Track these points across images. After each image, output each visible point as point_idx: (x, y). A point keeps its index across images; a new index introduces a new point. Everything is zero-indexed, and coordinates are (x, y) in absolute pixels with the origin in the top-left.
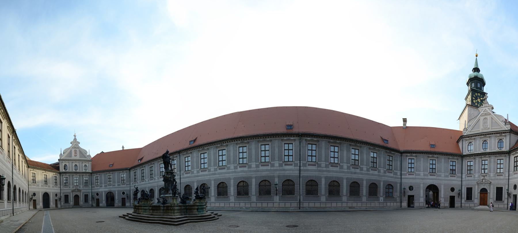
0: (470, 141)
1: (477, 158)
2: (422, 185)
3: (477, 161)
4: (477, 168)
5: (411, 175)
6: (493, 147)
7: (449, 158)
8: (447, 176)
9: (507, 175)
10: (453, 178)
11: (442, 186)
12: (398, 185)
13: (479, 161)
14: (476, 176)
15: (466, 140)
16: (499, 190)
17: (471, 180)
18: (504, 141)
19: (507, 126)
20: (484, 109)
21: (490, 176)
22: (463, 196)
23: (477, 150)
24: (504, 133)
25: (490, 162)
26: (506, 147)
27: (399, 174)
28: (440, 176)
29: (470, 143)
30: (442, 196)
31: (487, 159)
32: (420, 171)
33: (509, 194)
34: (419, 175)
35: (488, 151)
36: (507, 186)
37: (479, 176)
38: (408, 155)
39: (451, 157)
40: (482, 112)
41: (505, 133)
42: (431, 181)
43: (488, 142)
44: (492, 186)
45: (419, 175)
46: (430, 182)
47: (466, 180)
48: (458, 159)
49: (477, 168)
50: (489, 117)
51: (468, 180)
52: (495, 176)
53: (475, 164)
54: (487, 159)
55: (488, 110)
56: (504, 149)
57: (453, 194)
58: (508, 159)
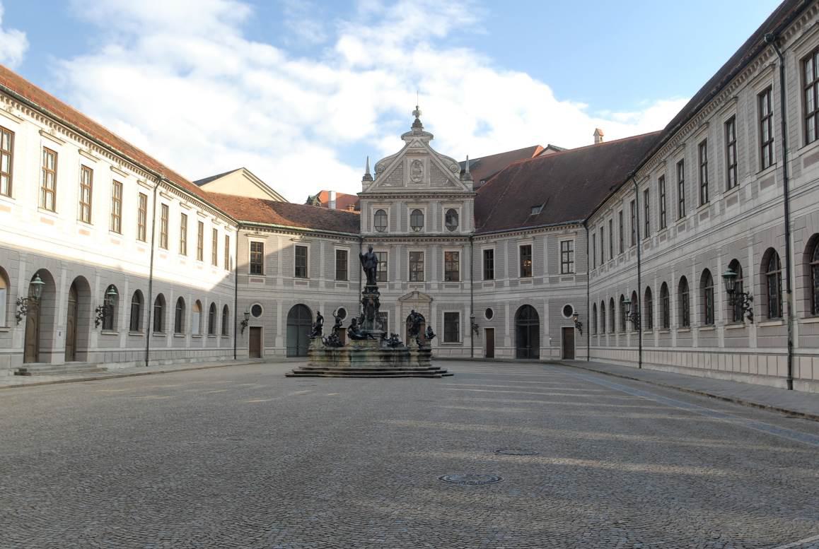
1: (398, 249)
7: (333, 244)
9: (469, 286)
16: (451, 320)
21: (428, 287)
33: (475, 328)
37: (404, 287)
44: (434, 310)
46: (296, 299)
52: (440, 287)
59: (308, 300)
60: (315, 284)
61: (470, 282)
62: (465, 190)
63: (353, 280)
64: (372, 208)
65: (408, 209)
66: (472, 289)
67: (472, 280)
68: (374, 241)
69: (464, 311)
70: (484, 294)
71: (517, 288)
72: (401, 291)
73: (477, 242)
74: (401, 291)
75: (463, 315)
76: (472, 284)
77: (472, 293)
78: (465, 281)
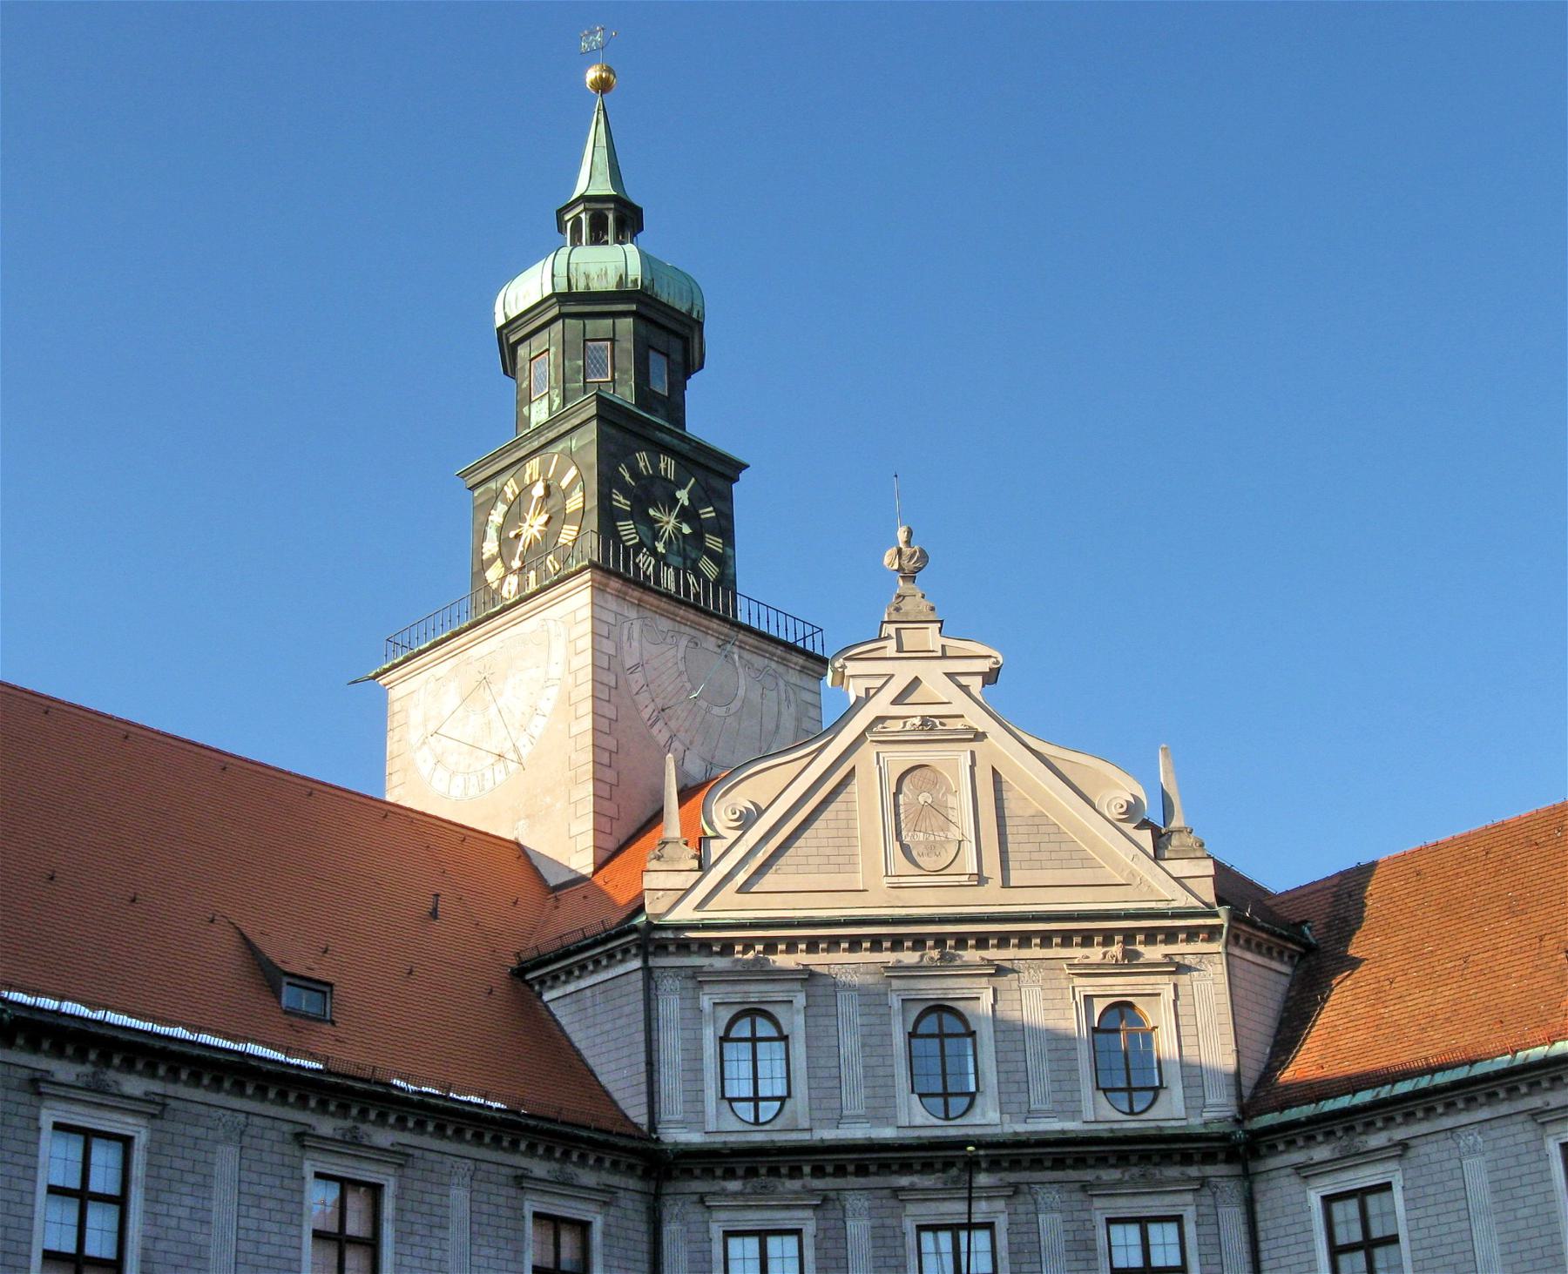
0: (755, 993)
1: (856, 1203)
3: (858, 1229)
7: (520, 1180)
15: (697, 978)
19: (1179, 868)
20: (904, 673)
23: (854, 1099)
29: (753, 1012)
35: (988, 1119)
38: (65, 1071)
39: (539, 1168)
40: (881, 705)
41: (1171, 936)
48: (607, 1197)
50: (953, 761)
55: (949, 691)
58: (1232, 1219)
62: (1183, 900)
64: (706, 1002)
68: (730, 1174)
73: (1273, 1162)
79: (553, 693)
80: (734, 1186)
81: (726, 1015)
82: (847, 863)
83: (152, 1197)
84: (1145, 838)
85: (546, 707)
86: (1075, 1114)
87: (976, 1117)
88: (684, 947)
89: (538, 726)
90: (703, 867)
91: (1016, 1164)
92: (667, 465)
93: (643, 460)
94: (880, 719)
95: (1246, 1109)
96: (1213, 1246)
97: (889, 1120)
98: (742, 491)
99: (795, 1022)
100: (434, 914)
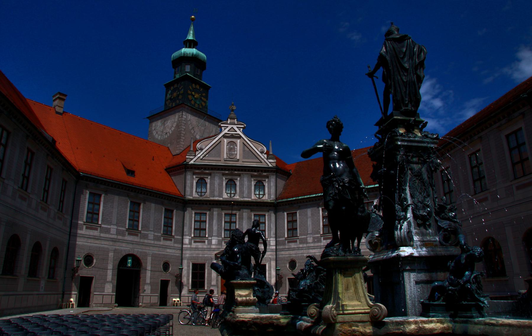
2: (111, 254)
3: (215, 213)
4: (215, 228)
5: (91, 229)
6: (246, 192)
8: (157, 238)
10: (168, 243)
11: (149, 259)
12: (65, 249)
13: (219, 216)
14: (214, 242)
17: (203, 249)
18: (266, 185)
22: (184, 280)
23: (216, 193)
24: (265, 172)
25: (241, 218)
26: (269, 194)
27: (68, 224)
28: (145, 237)
30: (148, 281)
31: (234, 212)
32: (110, 223)
34: (108, 231)
36: (273, 263)
40: (226, 131)
42: (131, 246)
43: (238, 183)
45: (108, 231)
46: (126, 248)
47: (191, 249)
49: (215, 228)
51: (196, 249)
53: (211, 219)
54: (234, 212)
55: (237, 129)
56: (266, 198)
57: (165, 276)
59: (137, 250)
60: (145, 237)
61: (274, 239)
62: (270, 165)
63: (177, 235)
64: (194, 177)
65: (224, 179)
66: (276, 245)
67: (276, 238)
69: (270, 264)
70: (289, 249)
71: (319, 244)
72: (218, 247)
74: (218, 247)
75: (270, 267)
76: (276, 240)
77: (276, 249)
78: (271, 239)
79: (175, 123)
80: (196, 205)
81: (198, 179)
82: (219, 156)
83: (104, 203)
84: (266, 156)
85: (174, 126)
86: (251, 198)
87: (235, 197)
88: (191, 168)
89: (173, 129)
90: (195, 156)
91: (240, 205)
92: (198, 87)
93: (194, 85)
94: (226, 133)
95: (277, 199)
96: (270, 220)
97: (222, 197)
98: (209, 91)
99: (208, 181)
100: (153, 160)
